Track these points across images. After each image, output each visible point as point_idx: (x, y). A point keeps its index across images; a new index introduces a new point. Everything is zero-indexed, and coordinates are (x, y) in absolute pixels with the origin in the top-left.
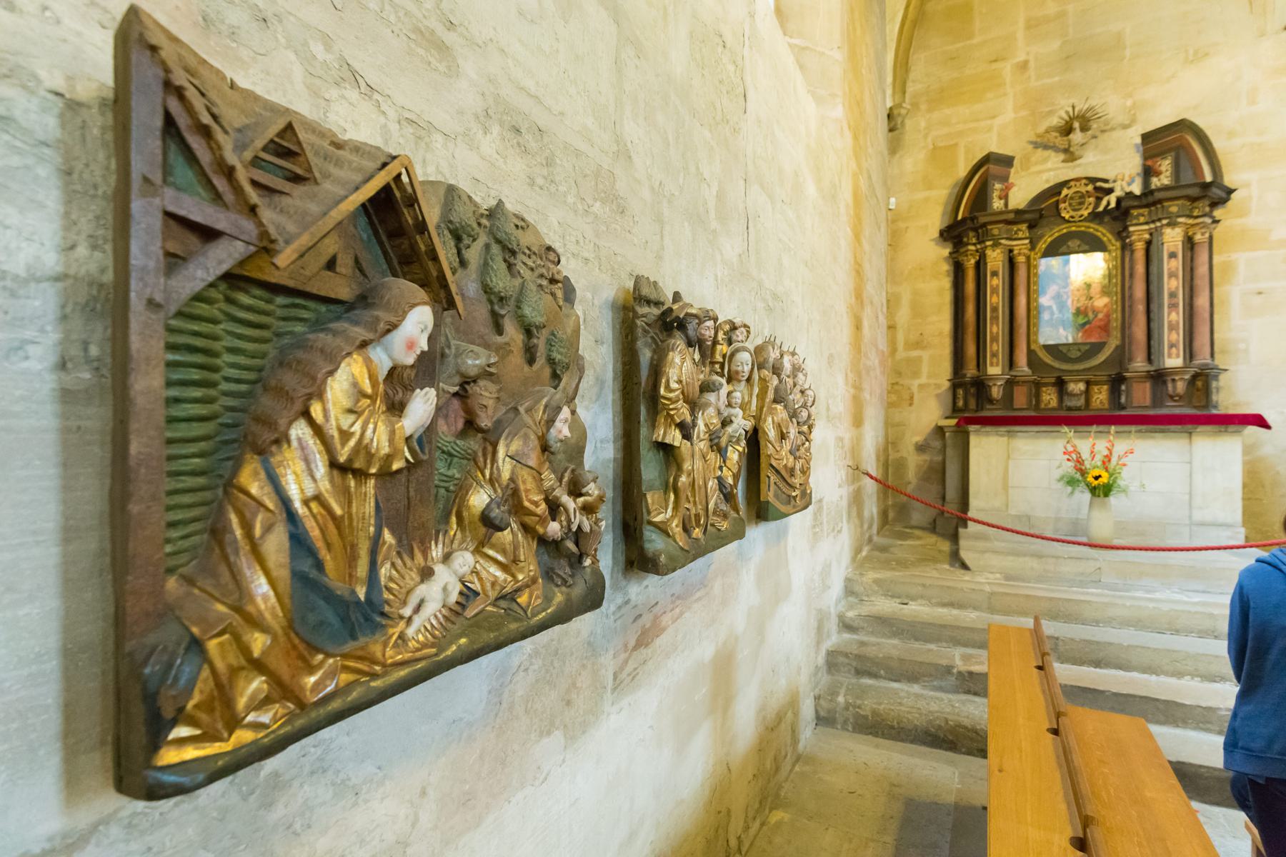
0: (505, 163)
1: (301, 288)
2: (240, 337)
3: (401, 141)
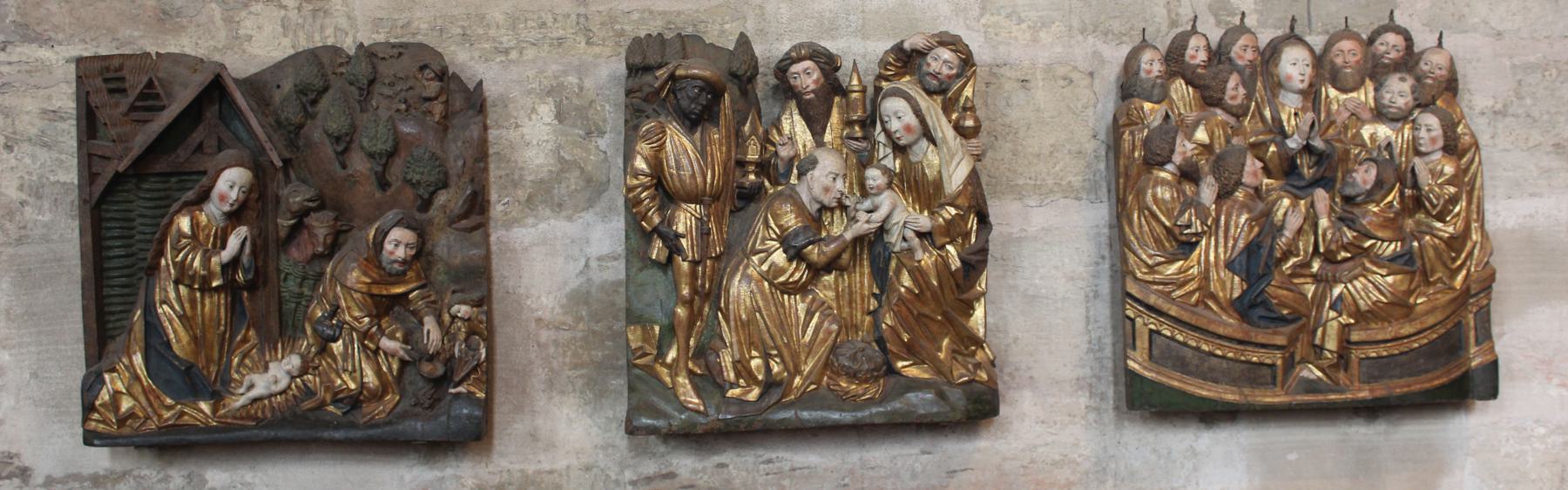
3: (300, 21)
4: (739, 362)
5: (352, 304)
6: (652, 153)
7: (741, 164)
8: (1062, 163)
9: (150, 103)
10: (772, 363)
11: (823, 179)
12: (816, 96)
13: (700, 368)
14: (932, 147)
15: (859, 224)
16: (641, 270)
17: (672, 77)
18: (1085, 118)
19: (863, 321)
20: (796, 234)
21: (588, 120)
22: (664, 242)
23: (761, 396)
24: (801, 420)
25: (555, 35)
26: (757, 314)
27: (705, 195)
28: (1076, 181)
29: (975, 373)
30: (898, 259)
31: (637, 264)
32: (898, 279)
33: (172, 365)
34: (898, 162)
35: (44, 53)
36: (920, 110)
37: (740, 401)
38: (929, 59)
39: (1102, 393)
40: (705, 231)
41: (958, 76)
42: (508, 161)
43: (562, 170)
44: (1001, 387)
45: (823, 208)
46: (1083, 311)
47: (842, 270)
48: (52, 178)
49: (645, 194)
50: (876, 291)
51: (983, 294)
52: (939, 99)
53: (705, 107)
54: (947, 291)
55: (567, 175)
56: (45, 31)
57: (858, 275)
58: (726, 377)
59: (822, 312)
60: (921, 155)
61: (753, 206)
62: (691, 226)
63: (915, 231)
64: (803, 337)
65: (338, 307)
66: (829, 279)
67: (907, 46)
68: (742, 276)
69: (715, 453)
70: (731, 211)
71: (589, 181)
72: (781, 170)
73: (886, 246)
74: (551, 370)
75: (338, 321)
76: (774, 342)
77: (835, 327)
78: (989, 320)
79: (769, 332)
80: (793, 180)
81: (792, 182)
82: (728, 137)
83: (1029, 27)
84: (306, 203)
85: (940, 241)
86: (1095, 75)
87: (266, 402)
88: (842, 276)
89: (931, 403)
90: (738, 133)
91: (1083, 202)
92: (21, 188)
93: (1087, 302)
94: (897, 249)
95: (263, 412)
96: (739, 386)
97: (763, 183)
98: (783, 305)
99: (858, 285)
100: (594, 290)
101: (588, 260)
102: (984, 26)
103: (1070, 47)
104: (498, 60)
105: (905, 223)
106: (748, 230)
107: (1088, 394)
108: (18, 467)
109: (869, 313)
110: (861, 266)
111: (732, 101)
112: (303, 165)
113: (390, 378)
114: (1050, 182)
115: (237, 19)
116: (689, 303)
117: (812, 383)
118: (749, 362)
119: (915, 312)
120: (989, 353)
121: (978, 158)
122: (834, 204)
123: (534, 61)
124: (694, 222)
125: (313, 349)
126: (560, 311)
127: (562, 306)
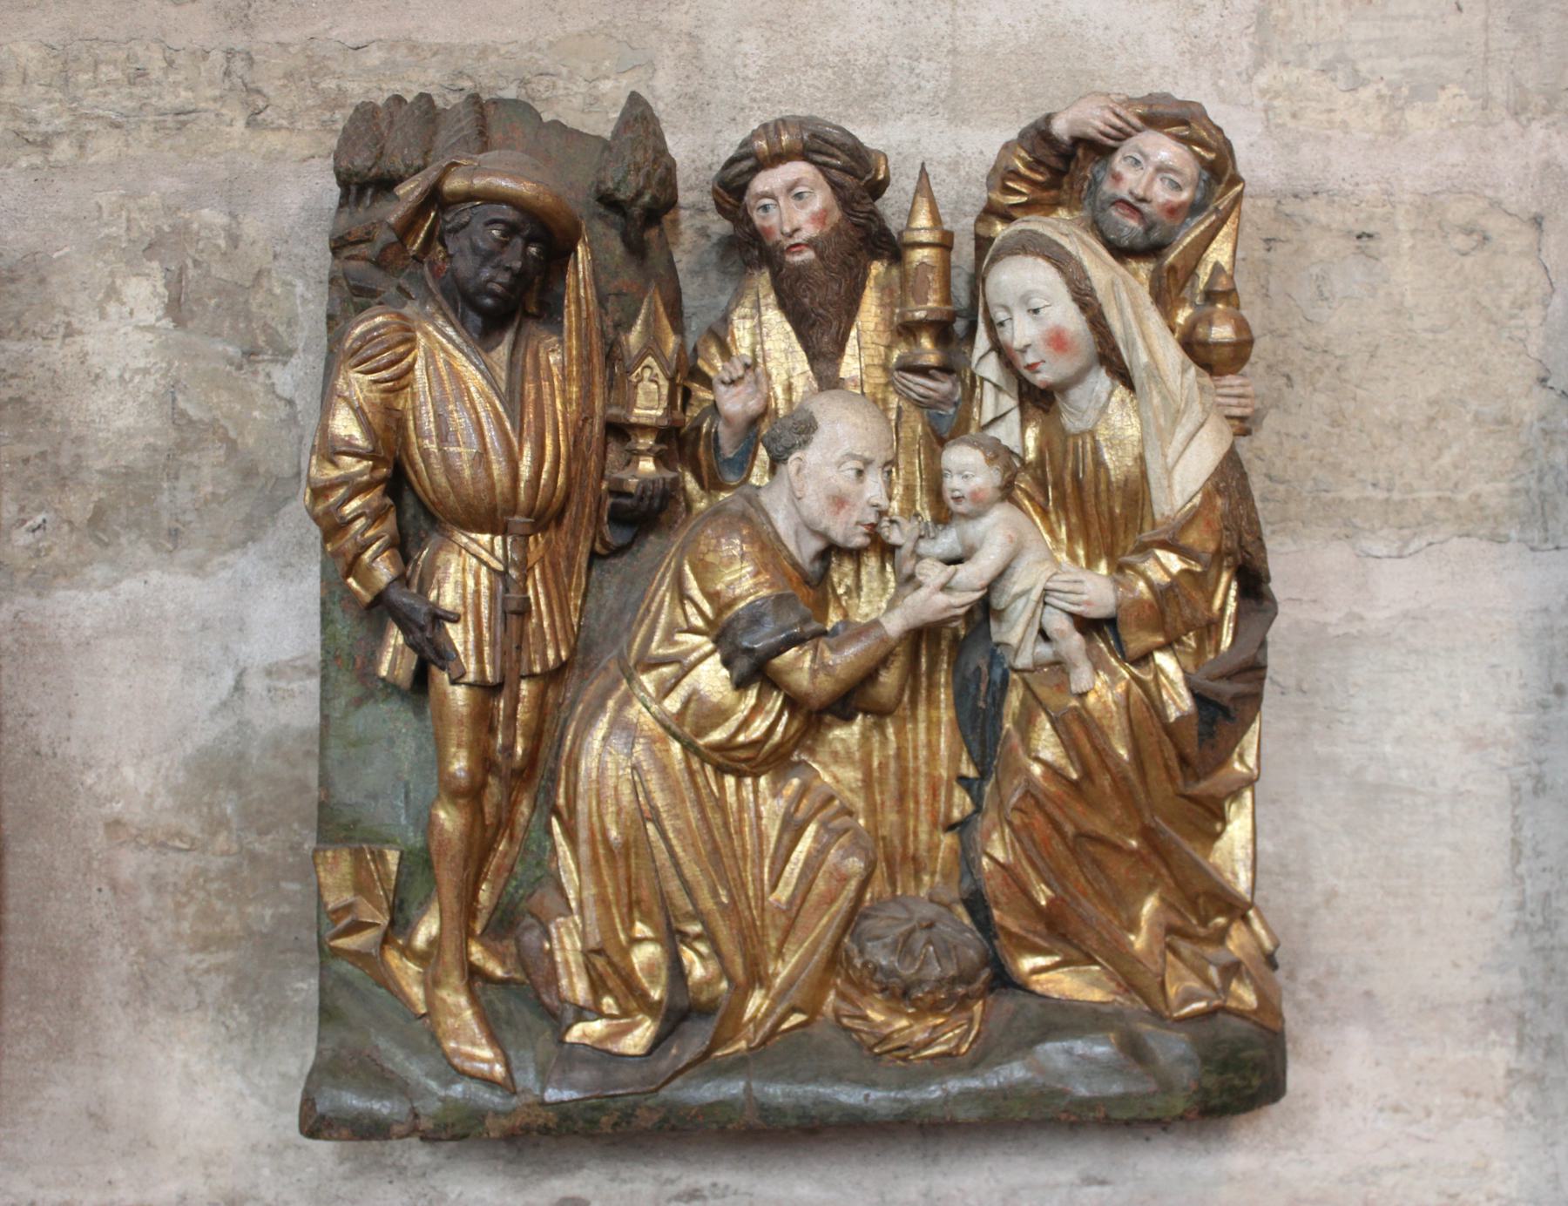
4: (599, 952)
6: (376, 397)
7: (619, 431)
8: (1455, 449)
10: (688, 955)
11: (829, 472)
12: (820, 255)
13: (503, 963)
14: (1121, 392)
15: (923, 593)
16: (359, 702)
17: (434, 198)
18: (1521, 334)
19: (933, 848)
20: (755, 617)
21: (248, 317)
22: (405, 631)
23: (658, 1043)
24: (765, 1110)
25: (170, 101)
26: (650, 827)
27: (514, 512)
28: (1493, 492)
29: (1225, 988)
30: (1027, 686)
31: (349, 689)
32: (1026, 739)
34: (1032, 434)
36: (1091, 292)
37: (601, 1056)
38: (1118, 163)
39: (1550, 1039)
40: (513, 606)
41: (1195, 208)
42: (47, 420)
43: (182, 446)
44: (1292, 1021)
45: (831, 551)
46: (1507, 826)
47: (880, 713)
49: (355, 503)
50: (969, 770)
51: (1250, 782)
52: (1144, 269)
53: (521, 278)
54: (1155, 773)
55: (194, 458)
57: (922, 726)
58: (567, 993)
59: (824, 825)
60: (1092, 415)
61: (652, 543)
62: (477, 592)
63: (1071, 615)
64: (774, 887)
66: (847, 735)
67: (1060, 128)
68: (612, 725)
69: (556, 1171)
70: (593, 556)
71: (248, 473)
72: (728, 449)
73: (995, 654)
74: (145, 952)
76: (695, 904)
77: (855, 864)
78: (1265, 845)
79: (681, 875)
80: (758, 476)
81: (754, 481)
82: (585, 360)
83: (1380, 97)
85: (1137, 641)
86: (1546, 225)
88: (882, 730)
89: (1109, 1069)
90: (612, 354)
91: (1510, 547)
93: (1515, 805)
94: (1023, 661)
96: (600, 1015)
97: (677, 484)
98: (721, 805)
99: (923, 753)
100: (254, 753)
101: (241, 675)
102: (1263, 92)
103: (1484, 149)
105: (1046, 592)
106: (633, 609)
107: (1513, 1041)
109: (950, 827)
110: (932, 702)
111: (596, 267)
114: (1427, 495)
116: (471, 795)
117: (793, 1010)
118: (626, 952)
119: (1069, 829)
120: (1262, 933)
121: (1244, 426)
122: (859, 540)
123: (113, 167)
124: (485, 581)
126: (169, 802)
127: (175, 791)
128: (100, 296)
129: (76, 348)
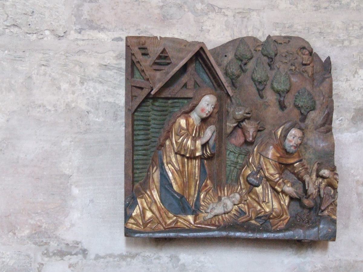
0: (297, 7)
1: (173, 96)
2: (155, 115)
5: (269, 167)
9: (163, 61)
33: (173, 196)
35: (101, 35)
42: (343, 98)
48: (104, 100)
56: (102, 24)
65: (262, 169)
75: (260, 176)
84: (245, 115)
87: (220, 217)
92: (88, 104)
95: (219, 222)
104: (338, 46)
108: (81, 249)
112: (238, 97)
113: (285, 207)
115: (202, 21)
125: (244, 191)
128: (354, 73)
129: (348, 84)
